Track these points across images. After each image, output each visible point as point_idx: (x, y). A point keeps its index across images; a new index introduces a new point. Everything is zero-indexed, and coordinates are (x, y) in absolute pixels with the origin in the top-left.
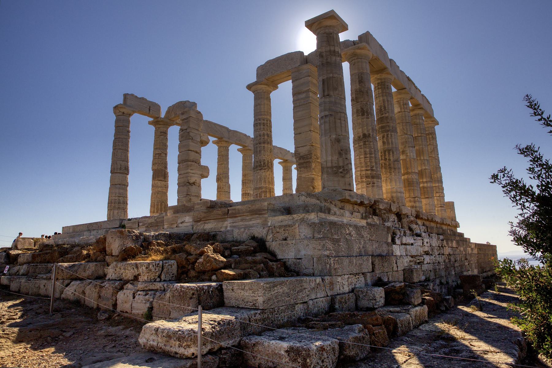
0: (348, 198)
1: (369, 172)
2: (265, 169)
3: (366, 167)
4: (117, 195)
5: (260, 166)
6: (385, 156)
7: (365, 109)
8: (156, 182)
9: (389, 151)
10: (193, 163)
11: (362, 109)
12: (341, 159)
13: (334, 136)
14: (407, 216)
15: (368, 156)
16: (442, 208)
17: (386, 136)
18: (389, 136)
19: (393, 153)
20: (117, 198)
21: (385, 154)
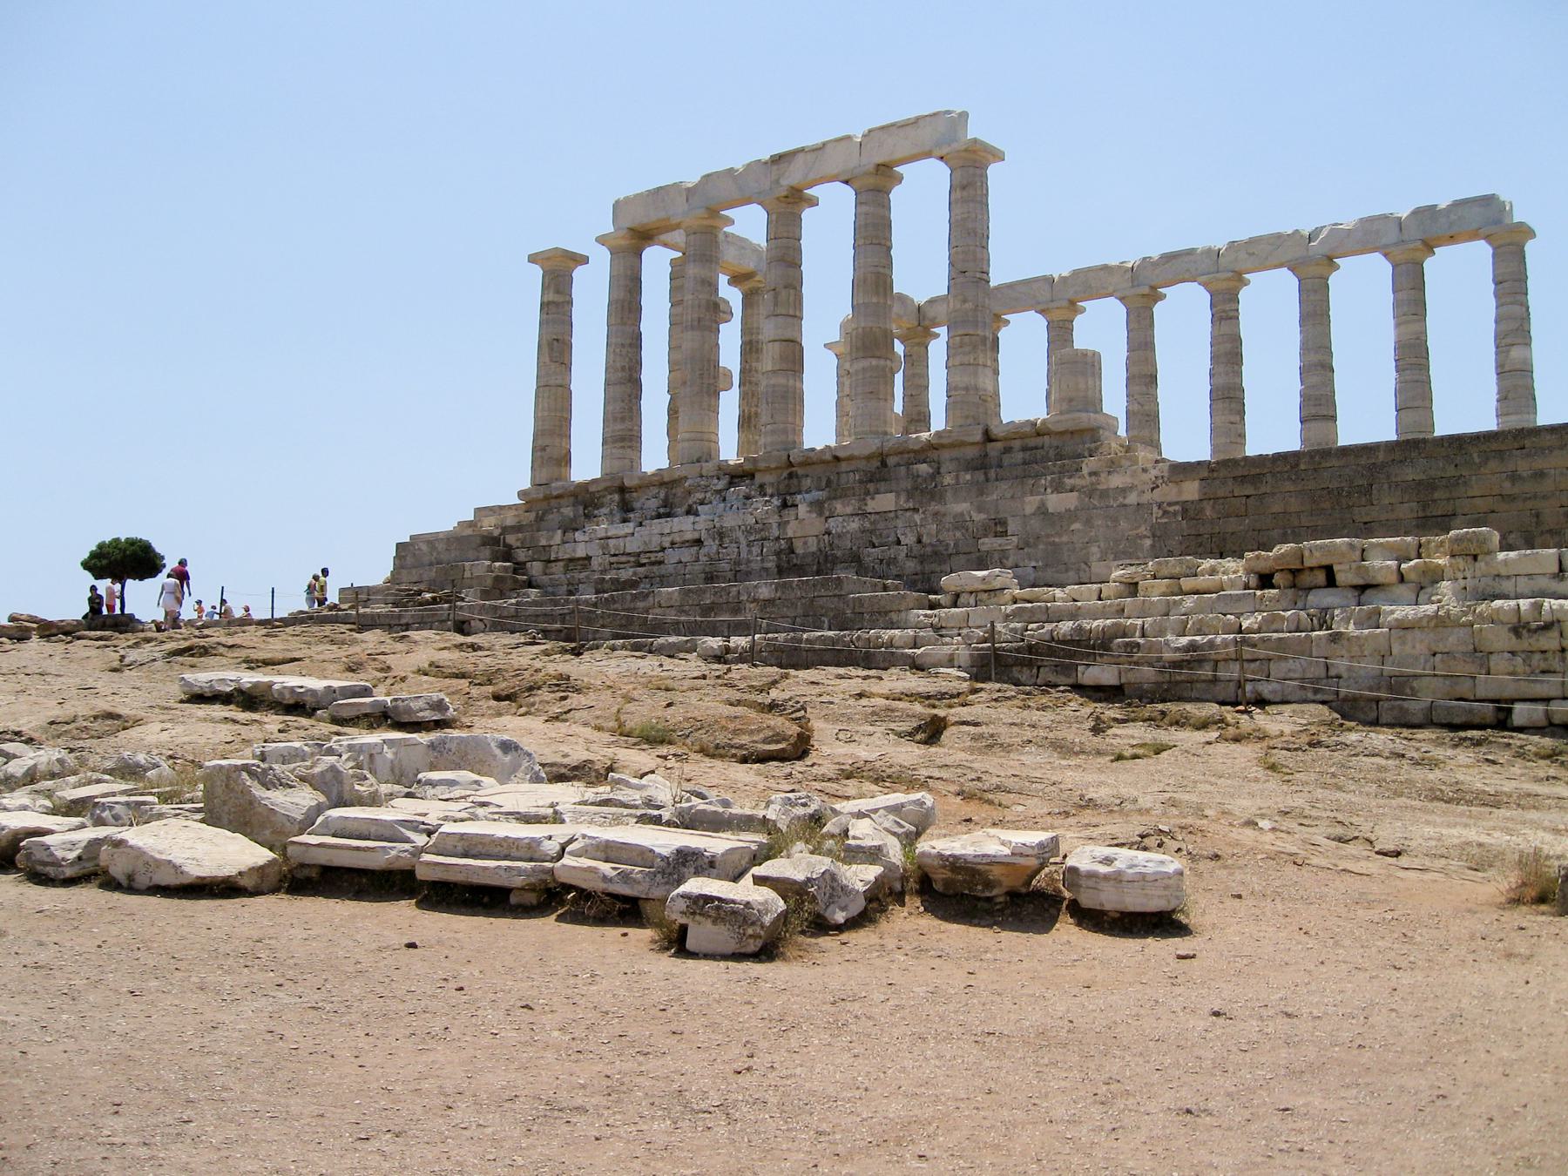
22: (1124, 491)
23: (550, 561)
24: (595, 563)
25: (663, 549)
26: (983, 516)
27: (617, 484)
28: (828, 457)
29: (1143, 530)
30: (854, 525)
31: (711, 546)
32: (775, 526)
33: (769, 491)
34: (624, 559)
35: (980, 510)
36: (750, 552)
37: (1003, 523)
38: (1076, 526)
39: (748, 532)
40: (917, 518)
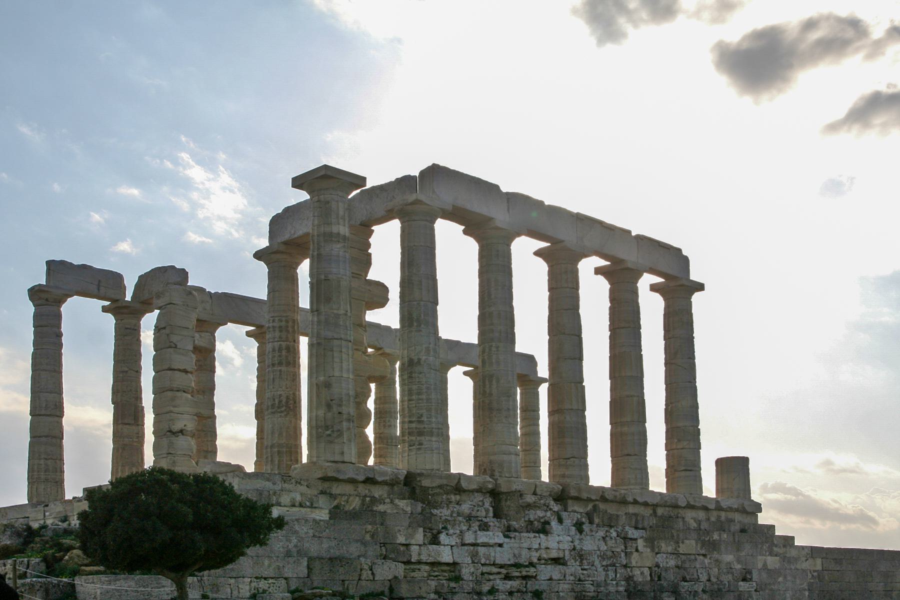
0: (330, 475)
1: (414, 425)
2: (282, 412)
3: (410, 417)
4: (43, 456)
5: (273, 405)
6: (484, 386)
7: (415, 316)
8: (120, 426)
9: (491, 376)
10: (179, 394)
11: (410, 314)
12: (329, 415)
13: (322, 378)
14: (521, 495)
15: (414, 397)
16: (688, 473)
17: (487, 350)
18: (494, 349)
19: (498, 381)
20: (42, 462)
21: (484, 382)
22: (796, 559)
23: (408, 562)
24: (466, 572)
25: (531, 564)
26: (739, 567)
27: (453, 483)
28: (630, 499)
29: (805, 586)
30: (672, 563)
31: (573, 567)
32: (623, 555)
33: (596, 520)
34: (495, 570)
35: (739, 562)
36: (607, 575)
37: (750, 573)
38: (781, 579)
39: (603, 557)
40: (707, 561)
